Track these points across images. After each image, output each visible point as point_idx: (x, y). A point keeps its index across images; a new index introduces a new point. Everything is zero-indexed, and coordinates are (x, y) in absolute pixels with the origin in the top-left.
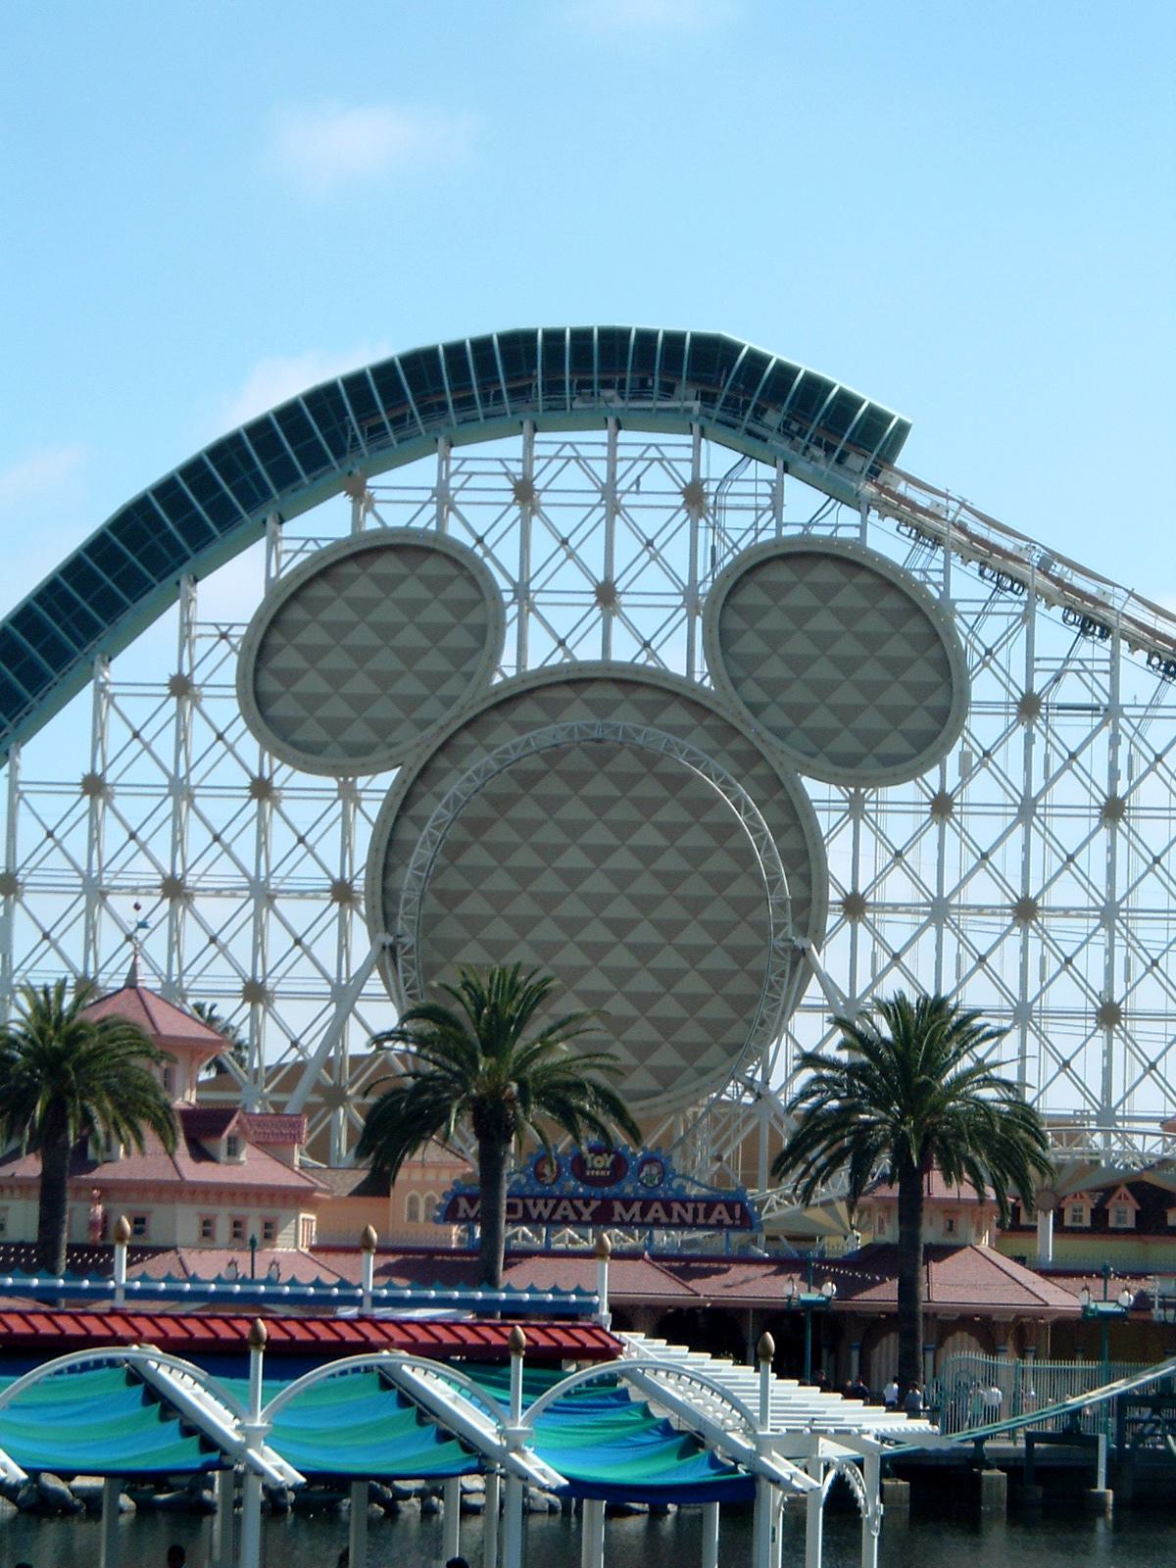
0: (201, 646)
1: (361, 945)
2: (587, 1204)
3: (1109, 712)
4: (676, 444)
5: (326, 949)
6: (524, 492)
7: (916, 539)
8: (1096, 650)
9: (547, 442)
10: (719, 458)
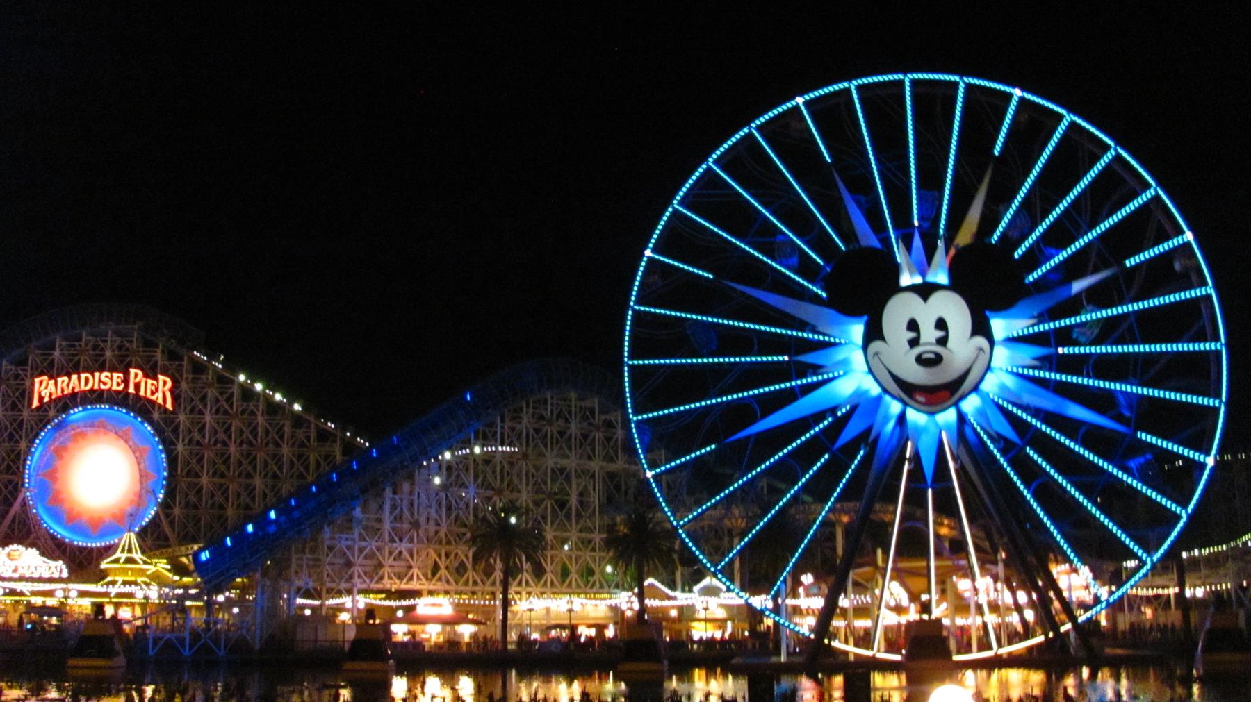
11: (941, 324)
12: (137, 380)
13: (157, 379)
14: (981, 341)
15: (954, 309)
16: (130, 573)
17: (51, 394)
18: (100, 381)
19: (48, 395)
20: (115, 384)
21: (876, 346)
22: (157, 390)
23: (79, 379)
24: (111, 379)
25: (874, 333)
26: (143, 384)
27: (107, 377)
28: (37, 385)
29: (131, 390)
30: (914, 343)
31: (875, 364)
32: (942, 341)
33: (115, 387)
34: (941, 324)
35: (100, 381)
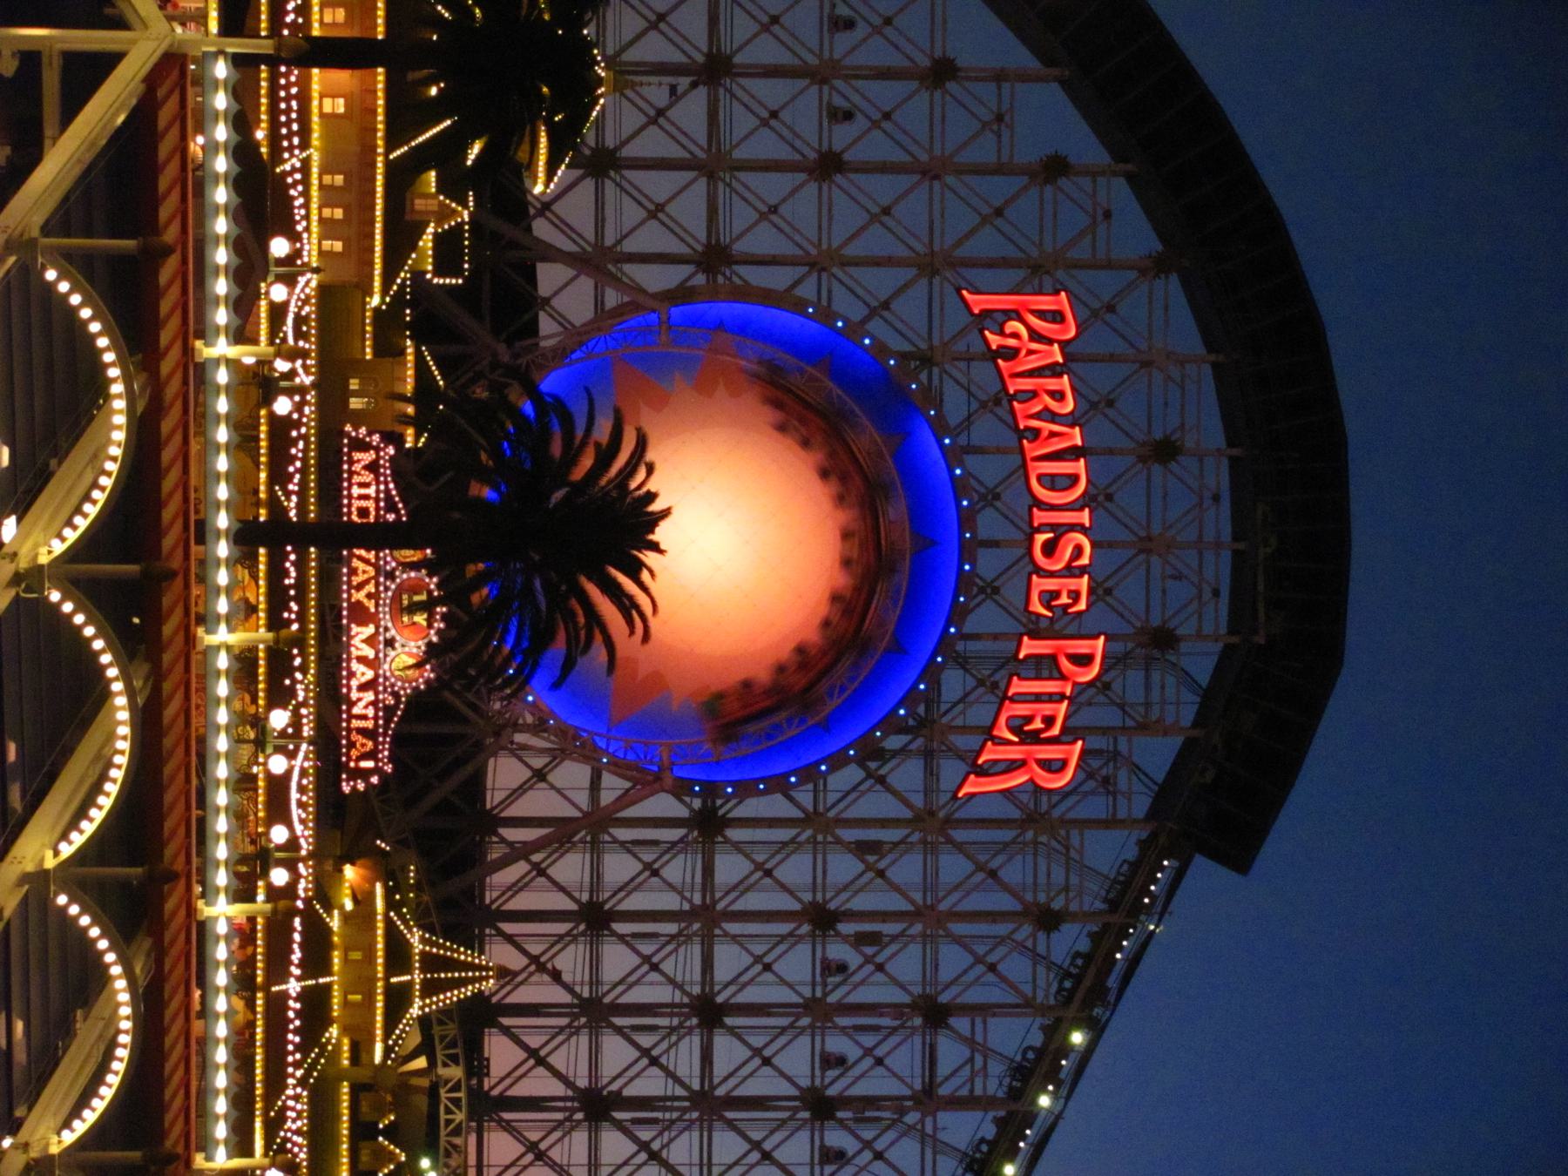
0: (987, 90)
1: (656, 279)
2: (369, 596)
4: (1217, 615)
5: (651, 239)
6: (1164, 451)
7: (1115, 881)
8: (994, 1083)
9: (1219, 476)
10: (1201, 663)
12: (1065, 664)
13: (1070, 733)
16: (356, 955)
17: (1011, 354)
18: (1060, 530)
19: (1012, 342)
20: (1051, 584)
22: (1035, 738)
23: (1074, 453)
24: (1071, 571)
26: (1051, 687)
27: (1079, 550)
28: (1045, 302)
29: (1029, 647)
33: (1040, 584)
35: (1060, 530)
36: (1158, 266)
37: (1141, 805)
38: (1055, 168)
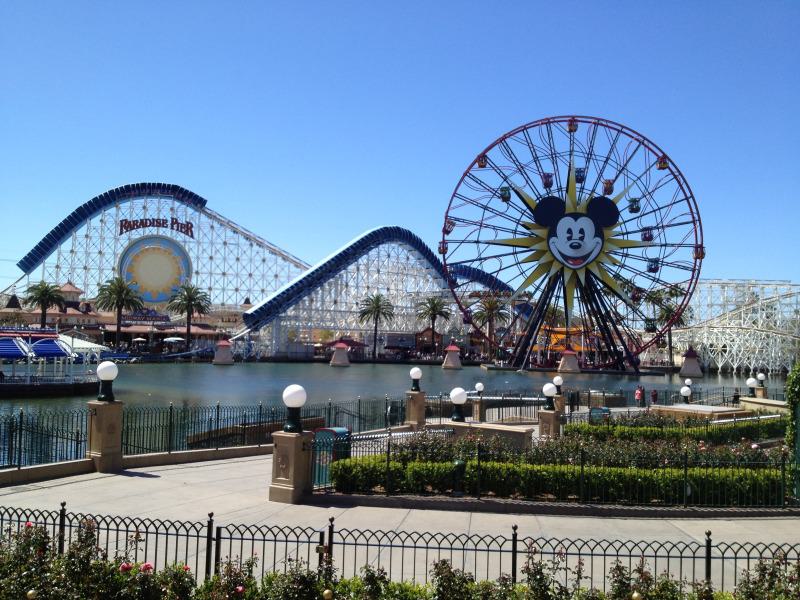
3: (238, 245)
4: (170, 201)
6: (144, 208)
10: (177, 204)
11: (582, 231)
14: (598, 240)
15: (586, 224)
21: (553, 239)
25: (553, 233)
30: (569, 239)
31: (552, 247)
32: (582, 239)
34: (582, 231)
36: (118, 208)
37: (197, 214)
38: (101, 221)
